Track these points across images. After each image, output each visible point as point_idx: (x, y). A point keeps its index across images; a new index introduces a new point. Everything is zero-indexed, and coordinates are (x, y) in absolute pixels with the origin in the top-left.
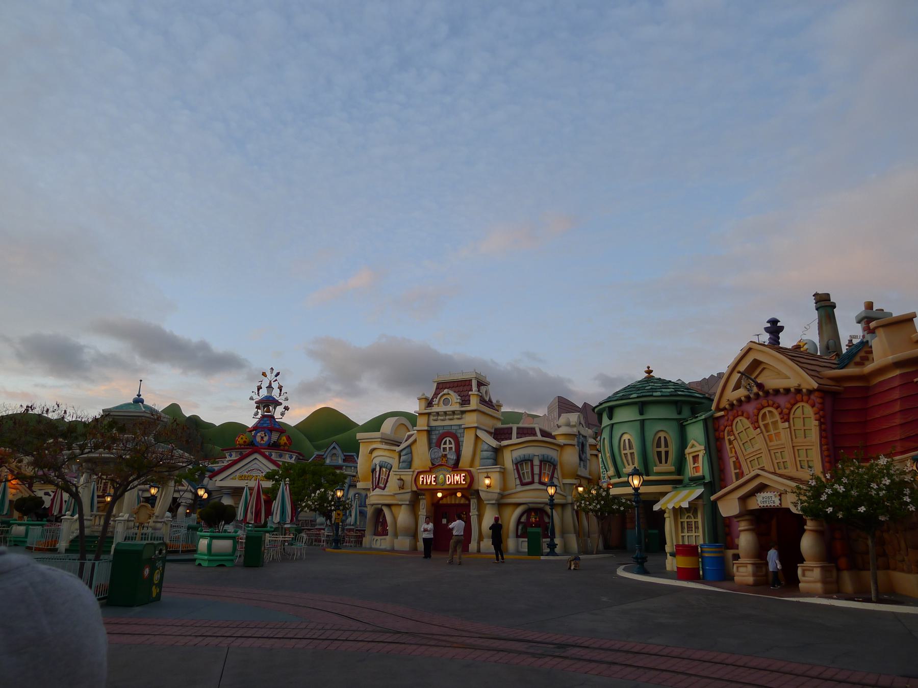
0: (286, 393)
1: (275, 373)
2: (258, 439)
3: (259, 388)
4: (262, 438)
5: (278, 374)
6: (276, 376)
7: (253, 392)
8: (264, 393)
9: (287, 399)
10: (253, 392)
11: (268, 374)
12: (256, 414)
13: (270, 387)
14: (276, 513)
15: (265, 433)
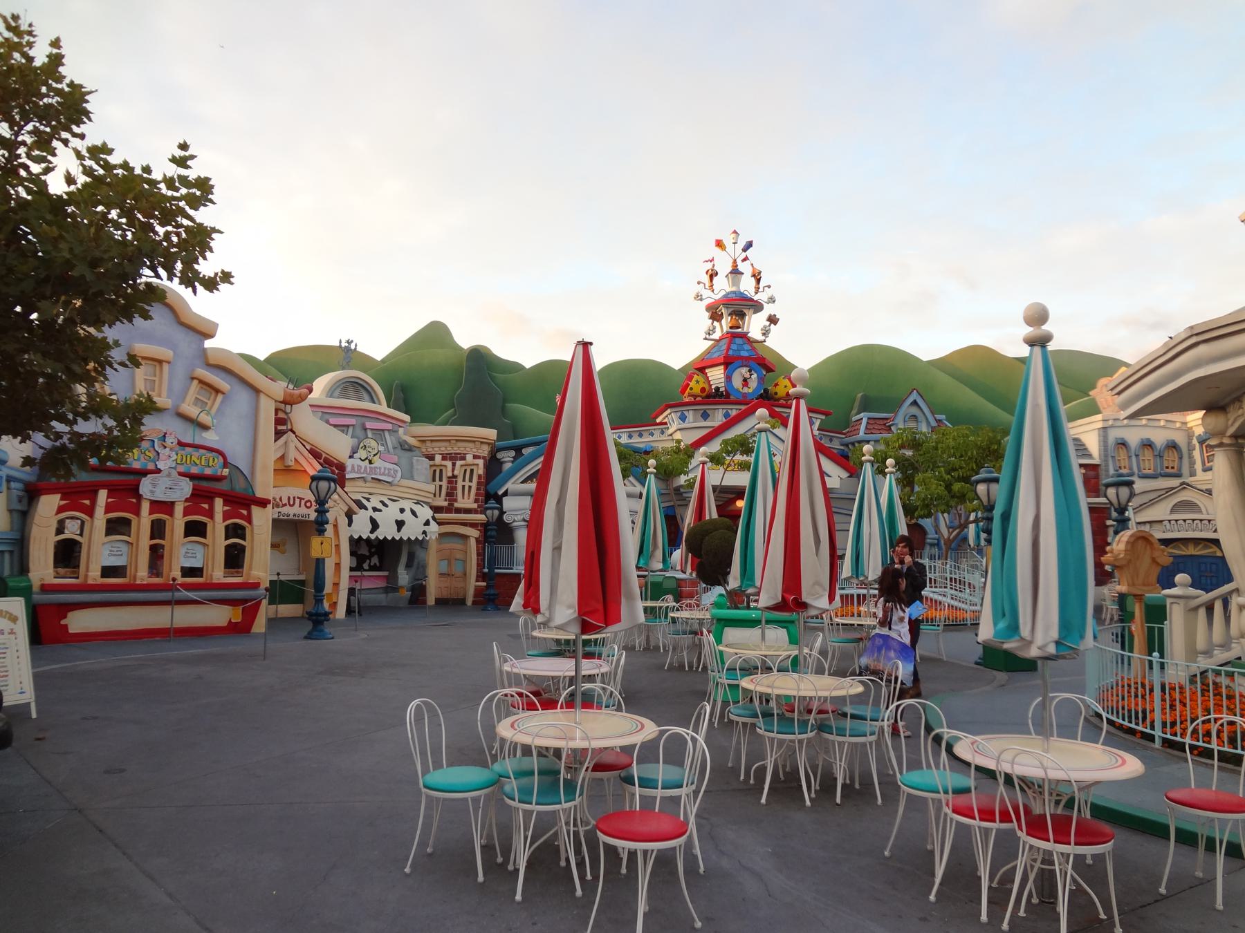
0: (769, 287)
1: (741, 244)
2: (737, 382)
3: (712, 275)
4: (745, 382)
5: (749, 245)
6: (745, 250)
7: (699, 283)
8: (723, 286)
9: (772, 300)
10: (699, 283)
11: (728, 242)
12: (710, 332)
13: (735, 272)
14: (557, 549)
15: (750, 371)
